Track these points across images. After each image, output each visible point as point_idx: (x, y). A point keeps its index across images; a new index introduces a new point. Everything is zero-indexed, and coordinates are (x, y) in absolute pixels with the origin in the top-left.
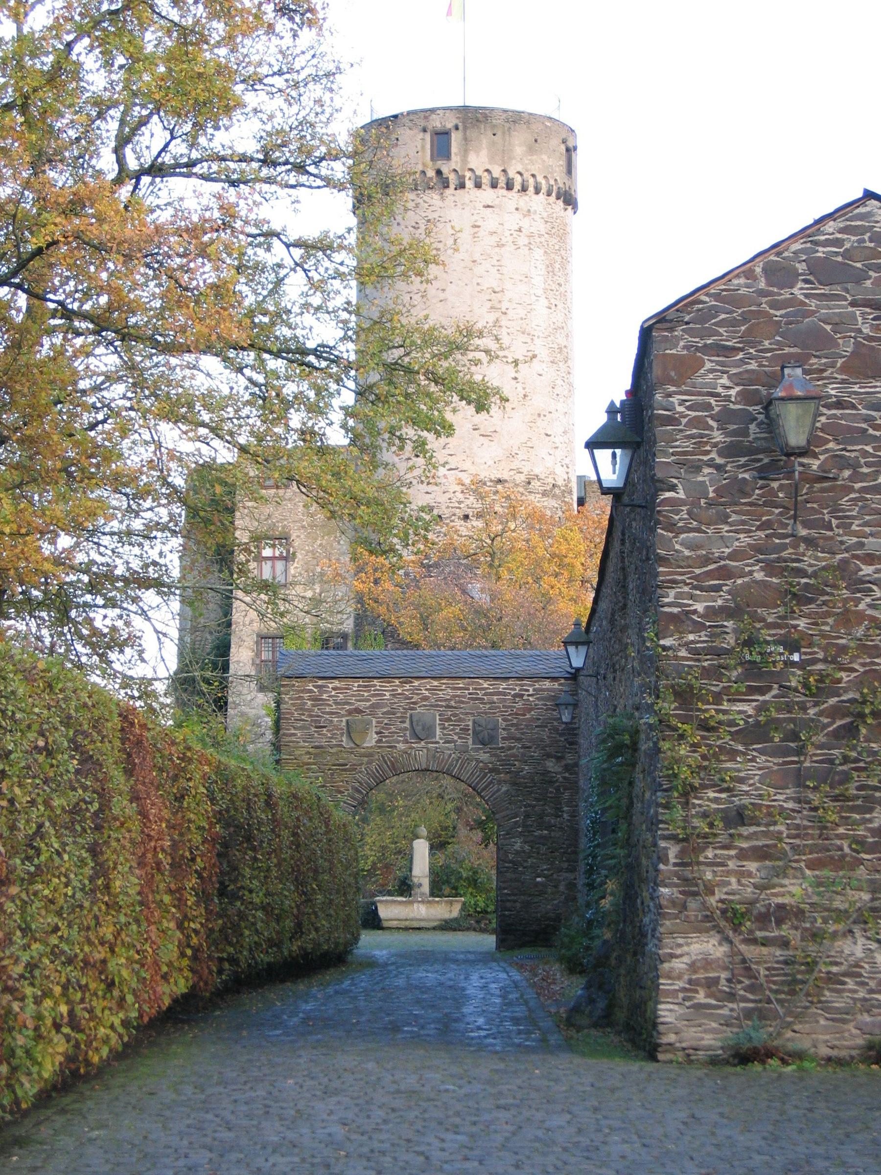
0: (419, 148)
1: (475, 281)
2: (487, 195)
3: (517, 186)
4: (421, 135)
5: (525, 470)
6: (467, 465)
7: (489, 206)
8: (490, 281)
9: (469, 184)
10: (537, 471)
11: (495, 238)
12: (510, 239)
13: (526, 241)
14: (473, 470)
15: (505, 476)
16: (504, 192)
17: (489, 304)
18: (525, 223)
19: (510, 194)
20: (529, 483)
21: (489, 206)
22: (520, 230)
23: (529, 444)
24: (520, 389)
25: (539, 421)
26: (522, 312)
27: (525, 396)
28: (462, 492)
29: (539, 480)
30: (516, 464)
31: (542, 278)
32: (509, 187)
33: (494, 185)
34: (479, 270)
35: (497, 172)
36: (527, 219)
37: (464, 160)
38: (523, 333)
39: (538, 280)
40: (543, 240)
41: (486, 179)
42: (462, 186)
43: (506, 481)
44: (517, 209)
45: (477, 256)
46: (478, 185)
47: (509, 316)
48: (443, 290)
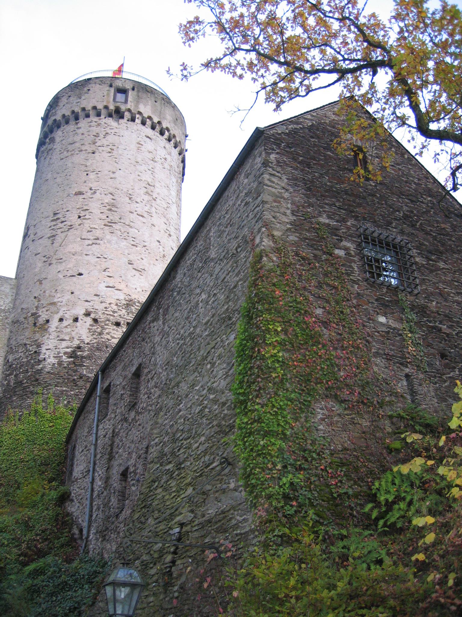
0: (105, 94)
1: (137, 173)
2: (148, 130)
4: (108, 88)
6: (122, 286)
7: (148, 137)
8: (147, 177)
9: (138, 121)
11: (150, 156)
14: (126, 290)
17: (145, 190)
21: (148, 137)
24: (161, 249)
28: (117, 305)
33: (153, 128)
35: (156, 120)
37: (137, 106)
38: (165, 217)
41: (149, 122)
42: (133, 120)
45: (139, 160)
48: (114, 173)
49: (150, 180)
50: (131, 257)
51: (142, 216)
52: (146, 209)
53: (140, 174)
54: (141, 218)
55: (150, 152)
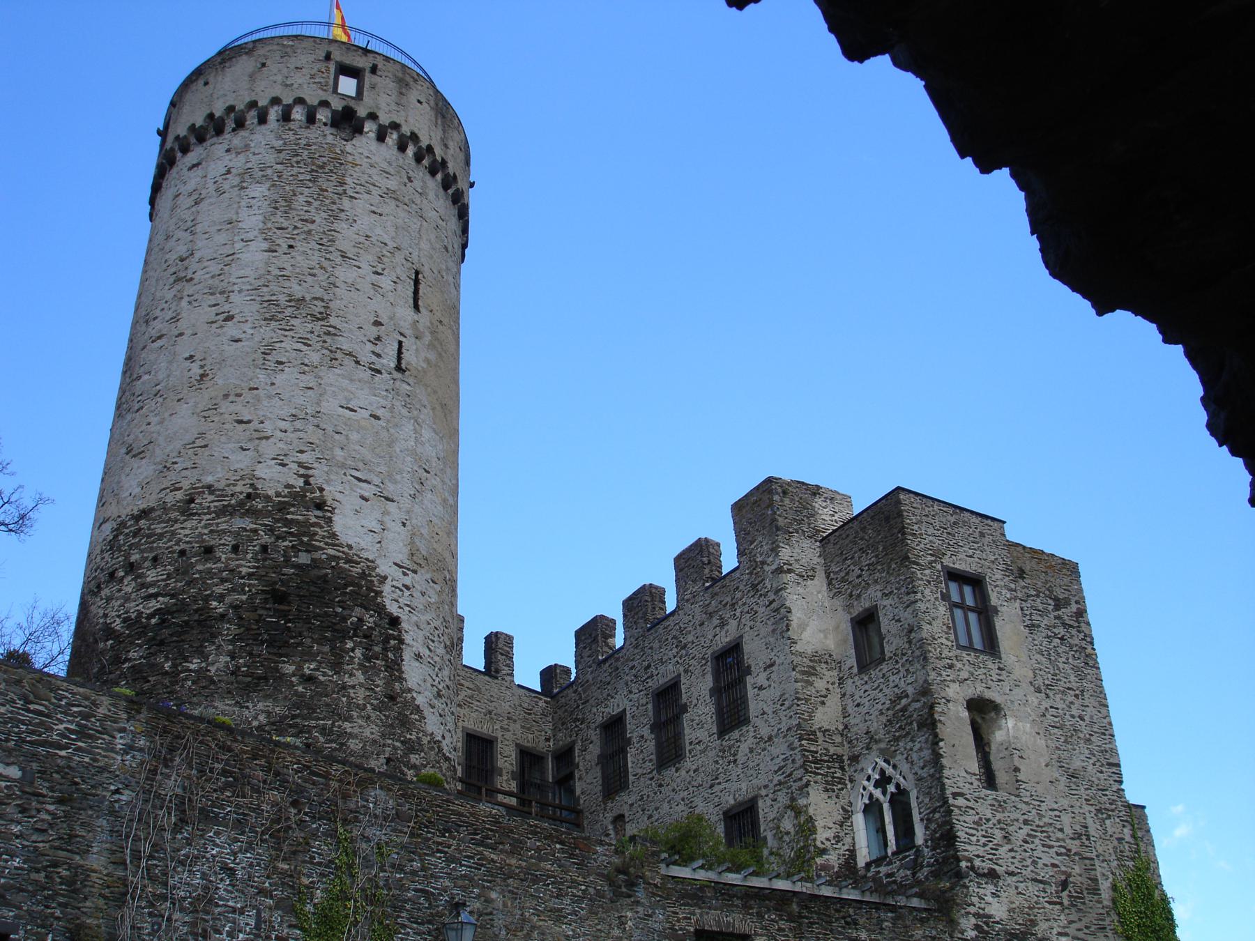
3: (230, 124)
5: (186, 484)
10: (209, 479)
11: (195, 196)
12: (212, 188)
13: (236, 181)
15: (151, 502)
16: (215, 140)
17: (172, 280)
18: (238, 163)
19: (220, 139)
20: (192, 501)
22: (229, 172)
23: (199, 443)
25: (225, 407)
26: (214, 268)
27: (202, 376)
29: (211, 493)
30: (172, 477)
31: (261, 218)
32: (219, 131)
34: (172, 243)
35: (199, 122)
36: (242, 158)
38: (212, 294)
39: (251, 221)
40: (269, 172)
43: (152, 509)
44: (228, 151)
46: (185, 150)
47: (195, 281)
49: (182, 250)
50: (130, 440)
51: (160, 337)
52: (170, 314)
53: (167, 256)
54: (159, 343)
55: (190, 195)
